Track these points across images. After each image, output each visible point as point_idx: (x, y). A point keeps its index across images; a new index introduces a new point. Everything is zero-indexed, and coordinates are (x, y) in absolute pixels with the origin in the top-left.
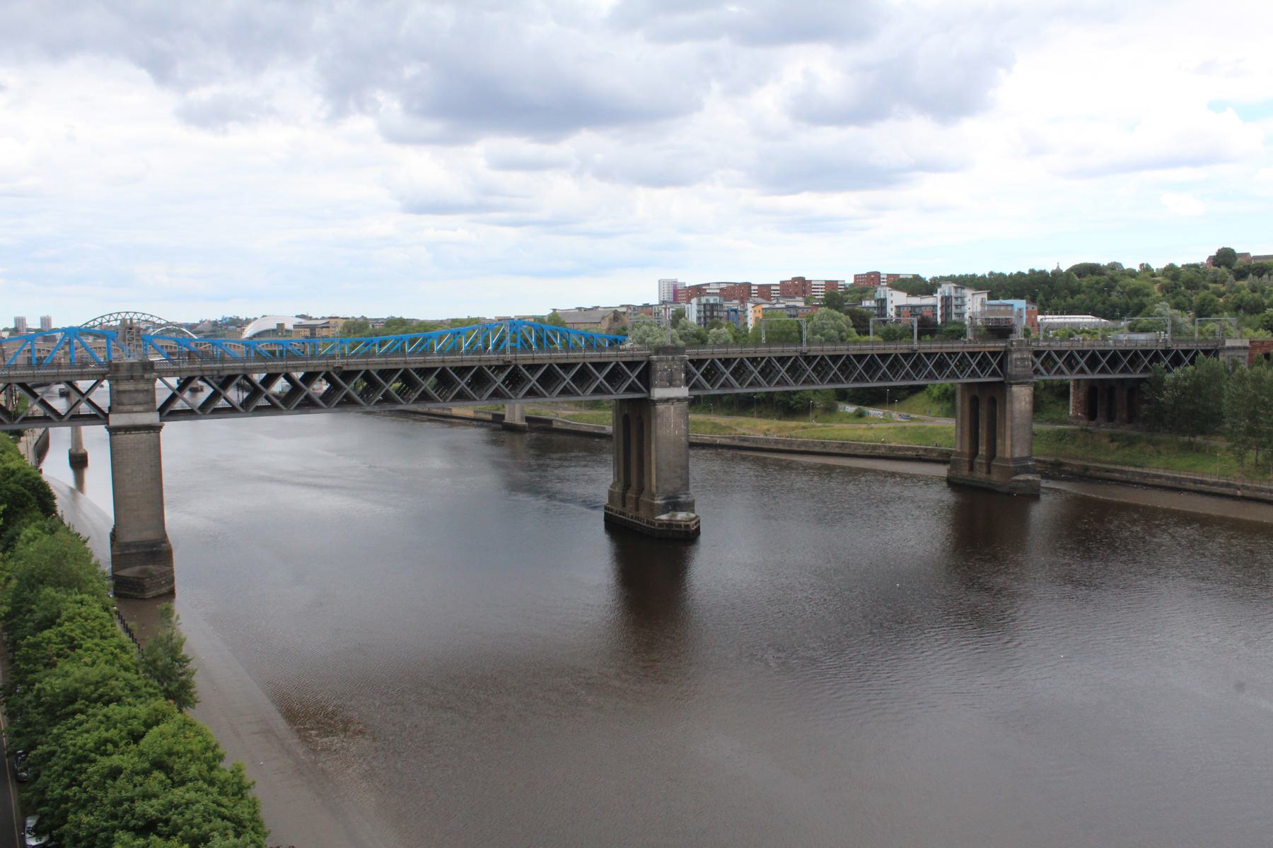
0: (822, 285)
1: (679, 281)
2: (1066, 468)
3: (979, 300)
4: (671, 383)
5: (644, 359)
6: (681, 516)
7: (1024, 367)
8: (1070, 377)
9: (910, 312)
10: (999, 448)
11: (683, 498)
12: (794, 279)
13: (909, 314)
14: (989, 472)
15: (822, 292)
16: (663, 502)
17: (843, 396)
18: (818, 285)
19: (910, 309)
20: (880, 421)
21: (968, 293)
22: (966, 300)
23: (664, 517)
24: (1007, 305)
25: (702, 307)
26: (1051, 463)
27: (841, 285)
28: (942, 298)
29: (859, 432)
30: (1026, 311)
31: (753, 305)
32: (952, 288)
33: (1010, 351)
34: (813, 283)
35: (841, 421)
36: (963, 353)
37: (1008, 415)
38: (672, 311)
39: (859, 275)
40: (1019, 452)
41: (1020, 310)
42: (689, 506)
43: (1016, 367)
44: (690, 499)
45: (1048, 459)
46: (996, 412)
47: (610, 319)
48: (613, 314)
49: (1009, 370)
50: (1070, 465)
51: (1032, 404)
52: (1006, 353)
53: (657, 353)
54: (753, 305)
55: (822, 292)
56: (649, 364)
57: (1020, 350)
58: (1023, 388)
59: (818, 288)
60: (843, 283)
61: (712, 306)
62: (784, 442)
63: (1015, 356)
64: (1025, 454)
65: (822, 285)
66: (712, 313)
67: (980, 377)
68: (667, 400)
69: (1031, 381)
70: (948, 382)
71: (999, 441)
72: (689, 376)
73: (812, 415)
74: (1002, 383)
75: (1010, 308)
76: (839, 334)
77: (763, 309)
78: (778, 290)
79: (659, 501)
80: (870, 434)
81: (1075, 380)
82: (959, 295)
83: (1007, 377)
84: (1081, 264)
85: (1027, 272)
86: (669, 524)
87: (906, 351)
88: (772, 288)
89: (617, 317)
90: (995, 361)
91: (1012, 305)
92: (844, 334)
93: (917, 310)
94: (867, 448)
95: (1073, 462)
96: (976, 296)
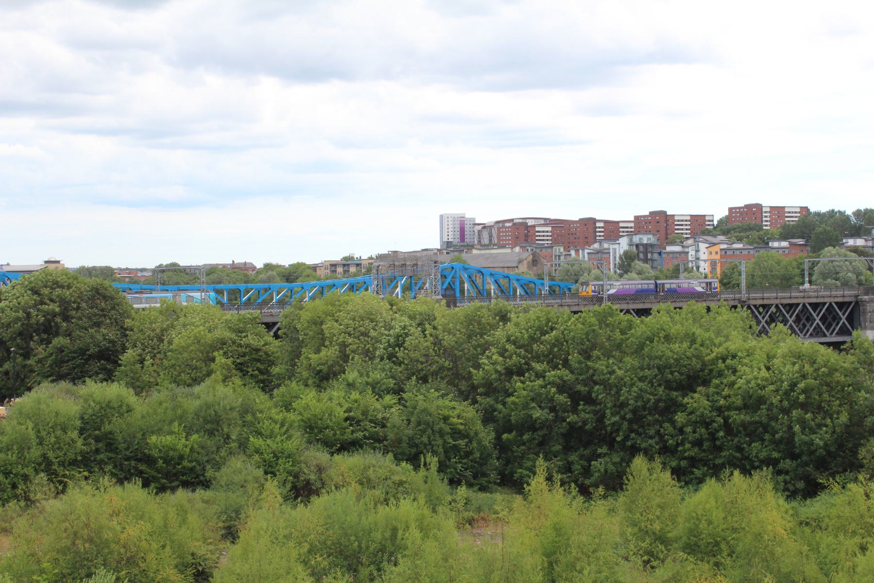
0: (686, 221)
15: (687, 229)
18: (682, 221)
25: (634, 247)
31: (707, 245)
36: (804, 305)
38: (588, 253)
39: (736, 208)
47: (529, 262)
54: (708, 245)
55: (687, 229)
59: (682, 225)
60: (710, 218)
61: (646, 246)
65: (686, 221)
67: (825, 336)
76: (857, 277)
77: (721, 250)
78: (631, 228)
88: (621, 225)
89: (536, 261)
90: (844, 315)
92: (862, 278)
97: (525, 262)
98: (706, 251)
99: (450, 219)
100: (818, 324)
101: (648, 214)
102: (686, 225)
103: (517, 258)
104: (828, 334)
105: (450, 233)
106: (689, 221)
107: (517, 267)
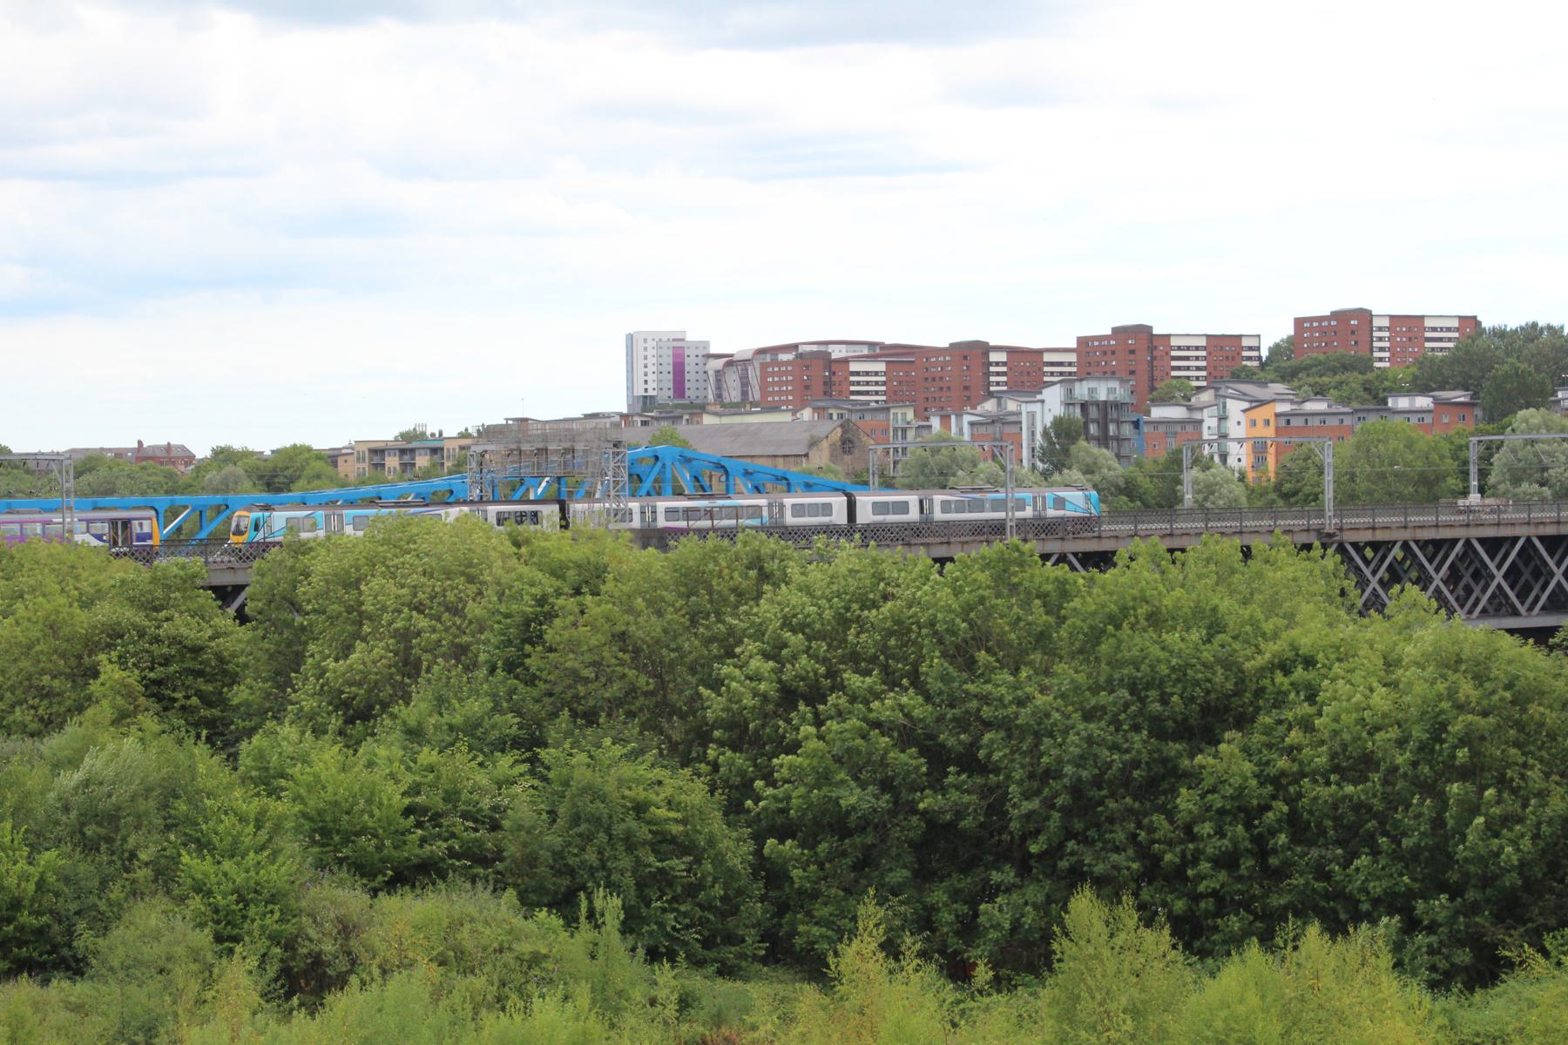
0: (1197, 348)
1: (691, 337)
15: (1198, 368)
18: (1188, 348)
25: (1078, 410)
31: (1246, 405)
34: (1174, 342)
36: (1468, 543)
38: (972, 424)
39: (1311, 319)
48: (839, 430)
54: (1246, 405)
55: (1198, 368)
59: (1187, 358)
60: (1254, 343)
61: (1104, 407)
65: (1197, 348)
67: (1516, 613)
77: (1277, 415)
78: (1070, 364)
88: (1047, 358)
89: (850, 441)
90: (1559, 564)
97: (825, 444)
98: (1242, 418)
99: (651, 344)
100: (1499, 586)
101: (1109, 332)
102: (1197, 358)
103: (806, 436)
104: (1522, 609)
105: (651, 377)
106: (1205, 348)
107: (806, 455)
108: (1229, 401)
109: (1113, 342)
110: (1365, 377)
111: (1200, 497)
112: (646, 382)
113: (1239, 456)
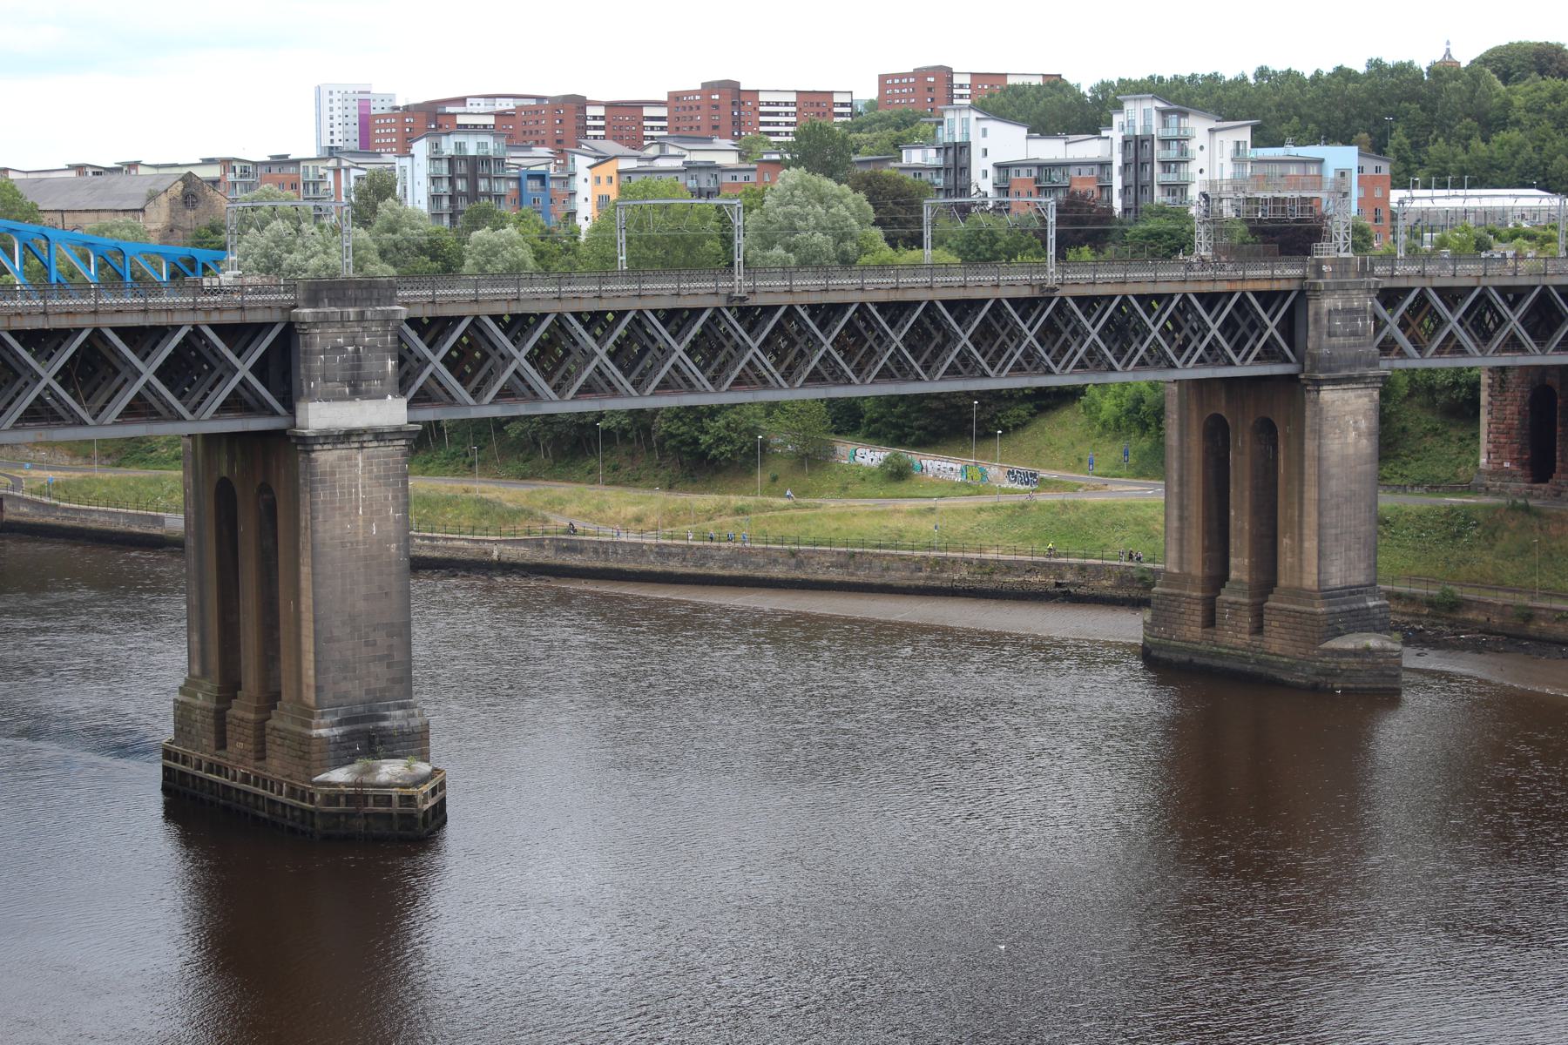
0: (787, 104)
1: (377, 89)
2: (1470, 616)
3: (1229, 148)
4: (356, 387)
5: (275, 316)
6: (390, 770)
7: (1354, 334)
8: (1481, 362)
9: (1037, 180)
10: (1286, 560)
11: (395, 720)
12: (709, 87)
13: (1033, 188)
14: (1258, 629)
15: (787, 124)
16: (337, 731)
17: (848, 419)
18: (777, 104)
19: (1035, 172)
20: (955, 489)
21: (1197, 127)
22: (1193, 146)
23: (340, 775)
24: (1306, 162)
25: (445, 165)
26: (1430, 603)
27: (843, 105)
28: (1125, 143)
29: (897, 523)
30: (1360, 179)
31: (592, 161)
32: (1154, 112)
33: (1316, 290)
34: (763, 97)
35: (844, 489)
37: (1310, 470)
38: (358, 178)
39: (893, 76)
40: (1338, 575)
41: (1343, 174)
42: (414, 742)
43: (1330, 335)
44: (415, 722)
45: (1419, 590)
46: (1275, 460)
47: (172, 200)
48: (180, 184)
49: (1310, 345)
50: (1485, 606)
51: (1375, 439)
52: (1304, 295)
53: (313, 300)
54: (592, 161)
55: (787, 124)
56: (290, 332)
57: (1341, 287)
58: (1351, 394)
59: (776, 114)
60: (847, 99)
62: (685, 553)
63: (1327, 303)
64: (1359, 577)
65: (787, 104)
66: (474, 185)
67: (1230, 363)
68: (347, 436)
69: (1371, 372)
70: (1140, 379)
71: (1285, 542)
72: (408, 365)
73: (761, 476)
74: (1291, 379)
75: (1313, 170)
76: (836, 245)
77: (620, 172)
79: (324, 730)
80: (926, 526)
81: (1491, 370)
82: (1172, 133)
83: (1308, 363)
84: (1510, 46)
85: (1361, 68)
86: (356, 796)
87: (1025, 293)
88: (647, 112)
89: (193, 196)
90: (1272, 319)
91: (1320, 162)
93: (1056, 175)
94: (918, 566)
95: (1489, 597)
96: (1219, 136)
97: (164, 199)
98: (587, 174)
99: (336, 96)
100: (1214, 337)
101: (699, 87)
102: (787, 114)
103: (145, 191)
104: (1178, 363)
105: (336, 129)
106: (795, 104)
107: (142, 210)
108: (576, 156)
109: (698, 97)
110: (899, 134)
111: (481, 259)
112: (332, 133)
113: (586, 214)
